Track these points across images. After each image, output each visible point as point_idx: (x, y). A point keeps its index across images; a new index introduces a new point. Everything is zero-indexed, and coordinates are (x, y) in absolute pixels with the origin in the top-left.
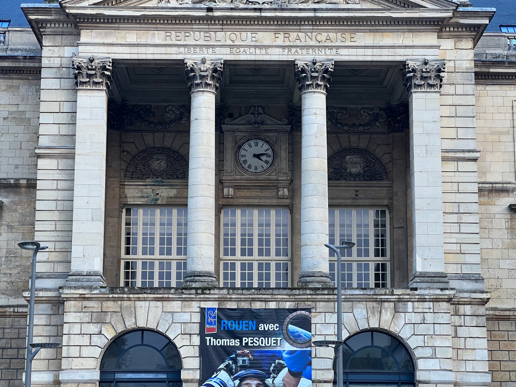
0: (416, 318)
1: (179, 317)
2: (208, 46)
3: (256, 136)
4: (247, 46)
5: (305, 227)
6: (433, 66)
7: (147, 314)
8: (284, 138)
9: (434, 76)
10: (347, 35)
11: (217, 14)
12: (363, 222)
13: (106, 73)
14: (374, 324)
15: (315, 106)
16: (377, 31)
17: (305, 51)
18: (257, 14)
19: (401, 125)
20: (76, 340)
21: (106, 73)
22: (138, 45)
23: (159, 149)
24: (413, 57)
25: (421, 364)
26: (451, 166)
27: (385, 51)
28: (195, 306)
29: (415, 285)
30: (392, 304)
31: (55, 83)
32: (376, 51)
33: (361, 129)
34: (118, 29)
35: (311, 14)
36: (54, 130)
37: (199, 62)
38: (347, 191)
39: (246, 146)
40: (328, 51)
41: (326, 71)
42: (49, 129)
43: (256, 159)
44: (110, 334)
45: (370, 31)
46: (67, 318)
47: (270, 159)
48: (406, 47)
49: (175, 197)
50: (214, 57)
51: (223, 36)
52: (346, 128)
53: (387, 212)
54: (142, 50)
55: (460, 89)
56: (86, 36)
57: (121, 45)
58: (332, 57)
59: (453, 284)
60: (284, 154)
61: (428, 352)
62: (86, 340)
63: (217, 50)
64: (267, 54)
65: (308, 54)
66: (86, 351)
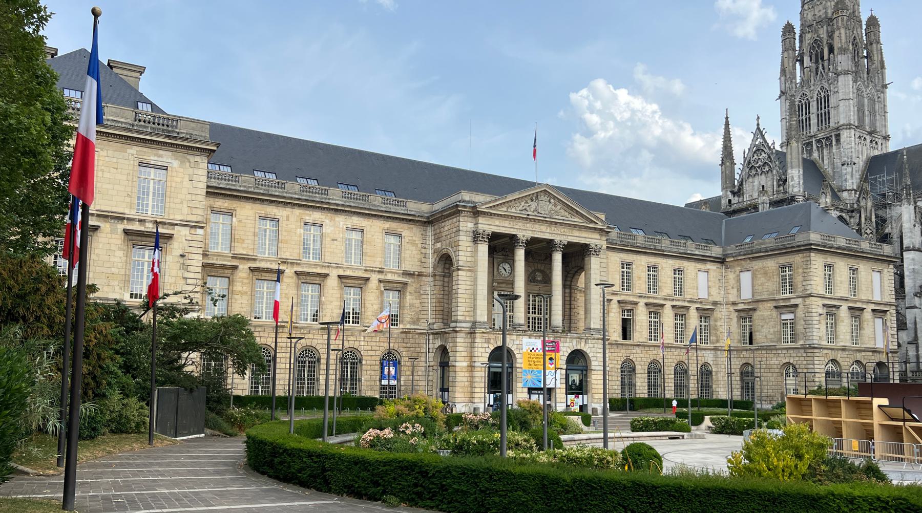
0: (591, 346)
5: (554, 307)
9: (597, 252)
20: (481, 350)
25: (593, 363)
36: (464, 259)
46: (477, 340)
51: (529, 226)
56: (481, 220)
62: (483, 350)
66: (484, 354)
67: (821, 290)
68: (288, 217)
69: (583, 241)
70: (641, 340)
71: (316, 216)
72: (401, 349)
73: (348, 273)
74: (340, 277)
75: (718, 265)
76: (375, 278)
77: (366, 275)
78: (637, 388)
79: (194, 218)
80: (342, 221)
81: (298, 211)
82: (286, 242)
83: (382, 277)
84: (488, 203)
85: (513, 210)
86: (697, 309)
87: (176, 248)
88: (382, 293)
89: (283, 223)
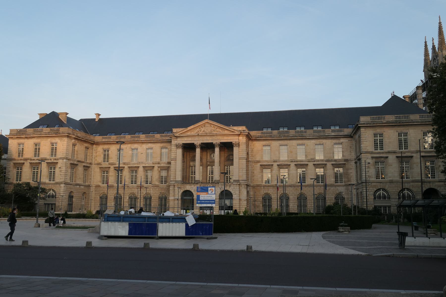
0: (233, 188)
6: (237, 142)
7: (188, 187)
26: (241, 160)
28: (196, 186)
31: (174, 147)
36: (174, 156)
42: (173, 156)
44: (182, 191)
51: (201, 138)
55: (243, 146)
56: (178, 139)
59: (241, 182)
67: (371, 148)
70: (292, 183)
71: (136, 146)
72: (167, 193)
73: (147, 165)
74: (143, 167)
75: (350, 139)
76: (156, 166)
77: (153, 165)
78: (290, 207)
79: (63, 156)
80: (145, 146)
81: (129, 145)
83: (159, 165)
84: (179, 132)
86: (332, 164)
87: (59, 165)
88: (160, 172)
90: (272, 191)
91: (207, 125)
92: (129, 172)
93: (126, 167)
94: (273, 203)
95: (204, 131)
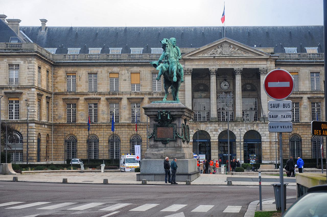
0: (261, 127)
1: (209, 128)
2: (214, 65)
3: (225, 80)
4: (223, 65)
8: (231, 81)
10: (246, 62)
11: (216, 58)
12: (251, 102)
13: (191, 72)
14: (252, 129)
15: (238, 79)
16: (252, 61)
17: (236, 66)
18: (225, 58)
19: (250, 104)
21: (191, 72)
22: (198, 65)
23: (201, 84)
24: (261, 67)
25: (262, 138)
27: (254, 66)
29: (261, 120)
30: (256, 124)
32: (252, 66)
33: (250, 78)
34: (194, 61)
35: (237, 57)
37: (212, 69)
38: (247, 93)
39: (222, 83)
40: (241, 66)
41: (241, 70)
43: (225, 86)
45: (251, 61)
47: (228, 86)
48: (259, 64)
49: (206, 96)
50: (215, 67)
51: (218, 63)
52: (246, 78)
53: (257, 99)
54: (199, 66)
56: (187, 63)
57: (194, 65)
58: (242, 67)
60: (231, 85)
61: (264, 135)
63: (216, 65)
64: (227, 66)
65: (237, 66)
68: (101, 71)
69: (254, 67)
71: (115, 69)
74: (128, 99)
77: (142, 97)
81: (106, 68)
82: (101, 84)
85: (206, 55)
89: (99, 75)
90: (302, 131)
91: (225, 45)
92: (108, 106)
93: (103, 98)
94: (303, 146)
95: (220, 53)
